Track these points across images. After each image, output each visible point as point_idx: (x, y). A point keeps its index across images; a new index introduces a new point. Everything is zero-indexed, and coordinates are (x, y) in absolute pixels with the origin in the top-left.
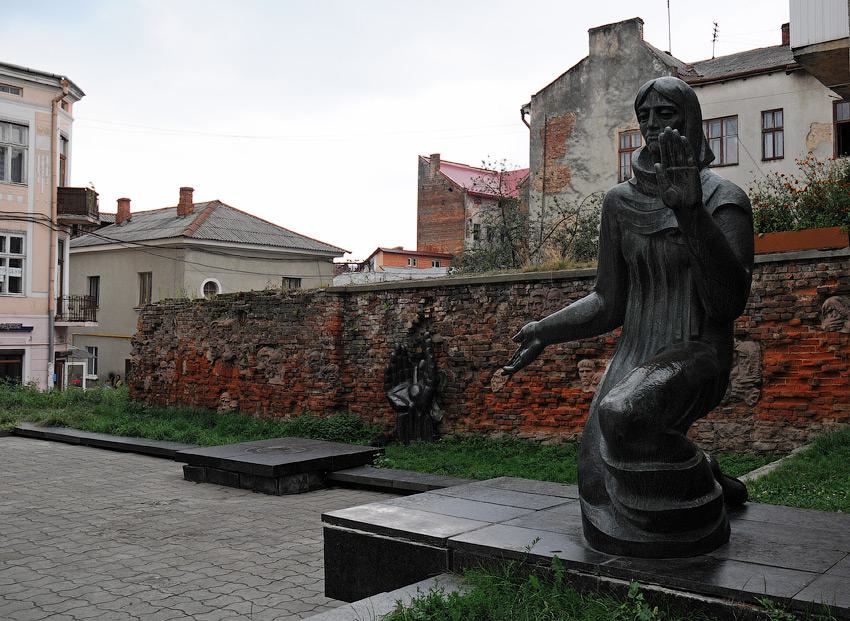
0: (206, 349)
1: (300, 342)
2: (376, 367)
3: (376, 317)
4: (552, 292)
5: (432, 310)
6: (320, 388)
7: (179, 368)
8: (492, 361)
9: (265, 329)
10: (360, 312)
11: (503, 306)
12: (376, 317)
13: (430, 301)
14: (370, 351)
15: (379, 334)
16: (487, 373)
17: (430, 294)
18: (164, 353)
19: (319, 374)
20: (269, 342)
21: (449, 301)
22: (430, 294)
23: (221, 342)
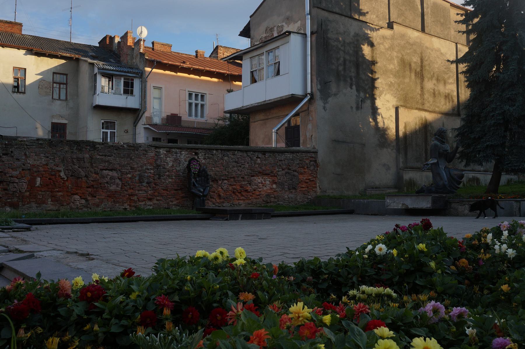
0: (60, 171)
1: (132, 168)
2: (170, 180)
3: (171, 159)
4: (245, 155)
5: (198, 157)
6: (145, 190)
7: (31, 183)
8: (222, 178)
9: (108, 161)
10: (162, 156)
11: (226, 158)
12: (171, 159)
13: (196, 154)
14: (167, 173)
15: (173, 166)
16: (220, 182)
17: (197, 151)
18: (15, 173)
19: (145, 184)
20: (110, 167)
21: (205, 154)
22: (197, 151)
23: (76, 167)
